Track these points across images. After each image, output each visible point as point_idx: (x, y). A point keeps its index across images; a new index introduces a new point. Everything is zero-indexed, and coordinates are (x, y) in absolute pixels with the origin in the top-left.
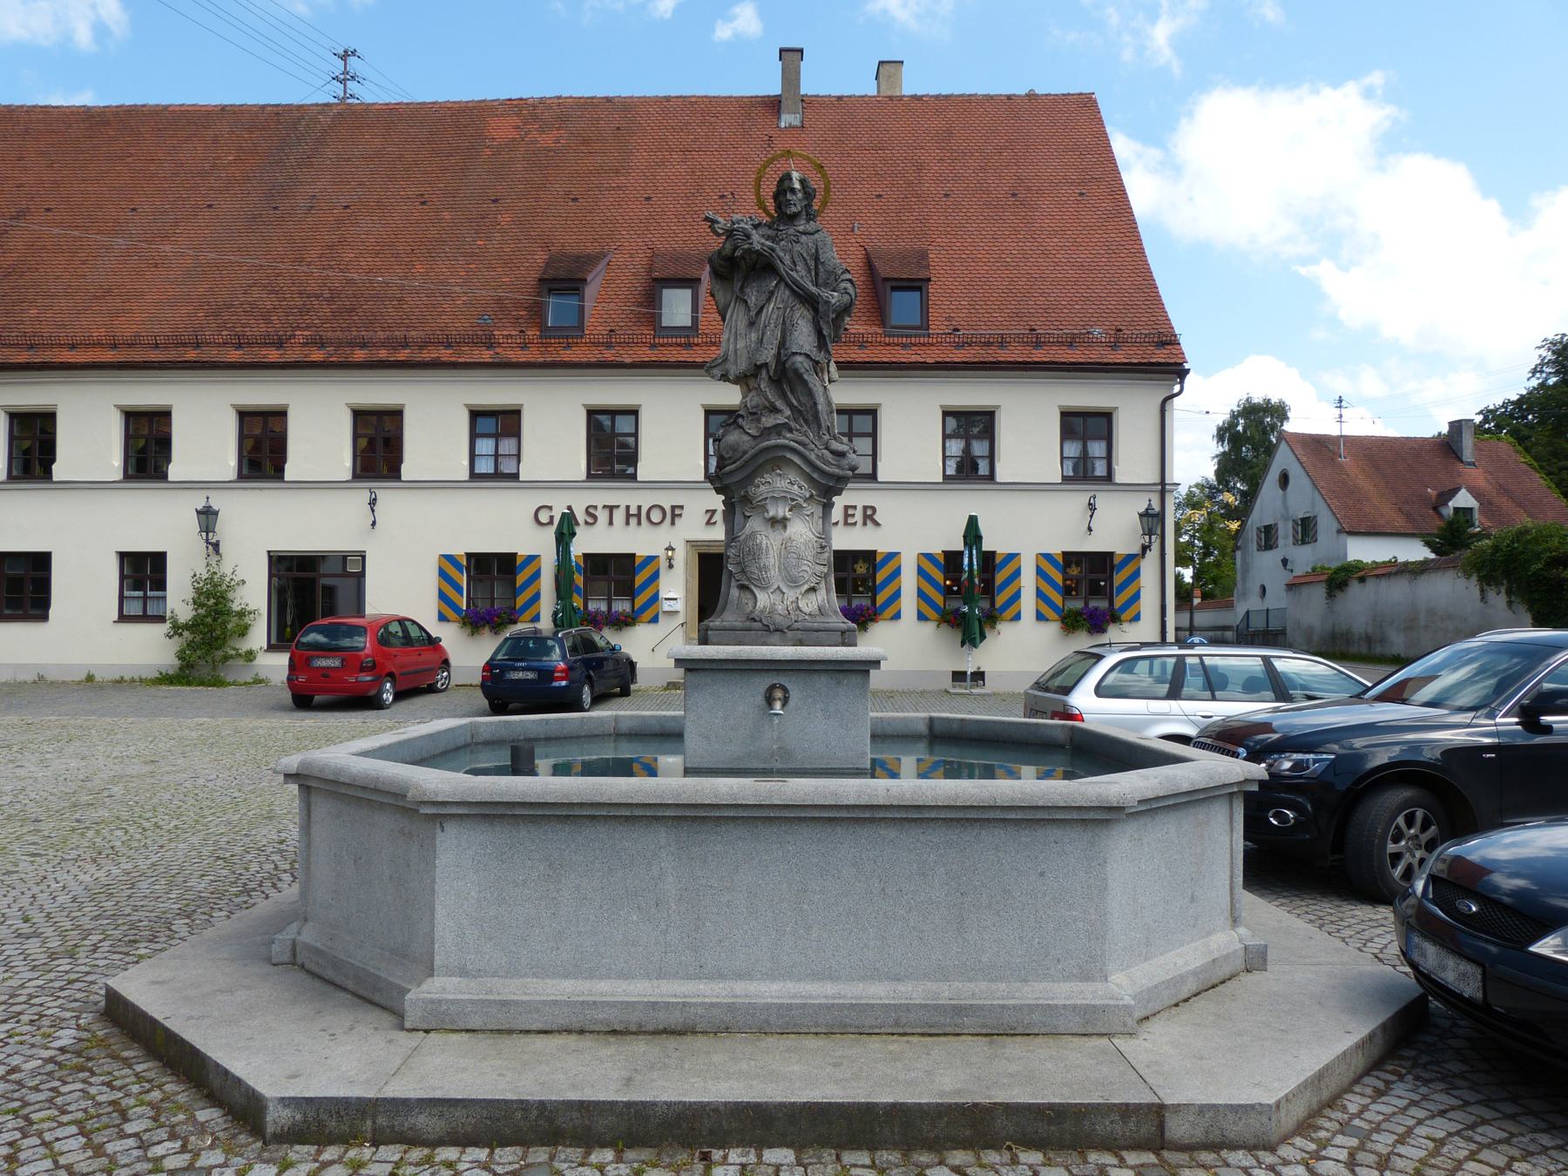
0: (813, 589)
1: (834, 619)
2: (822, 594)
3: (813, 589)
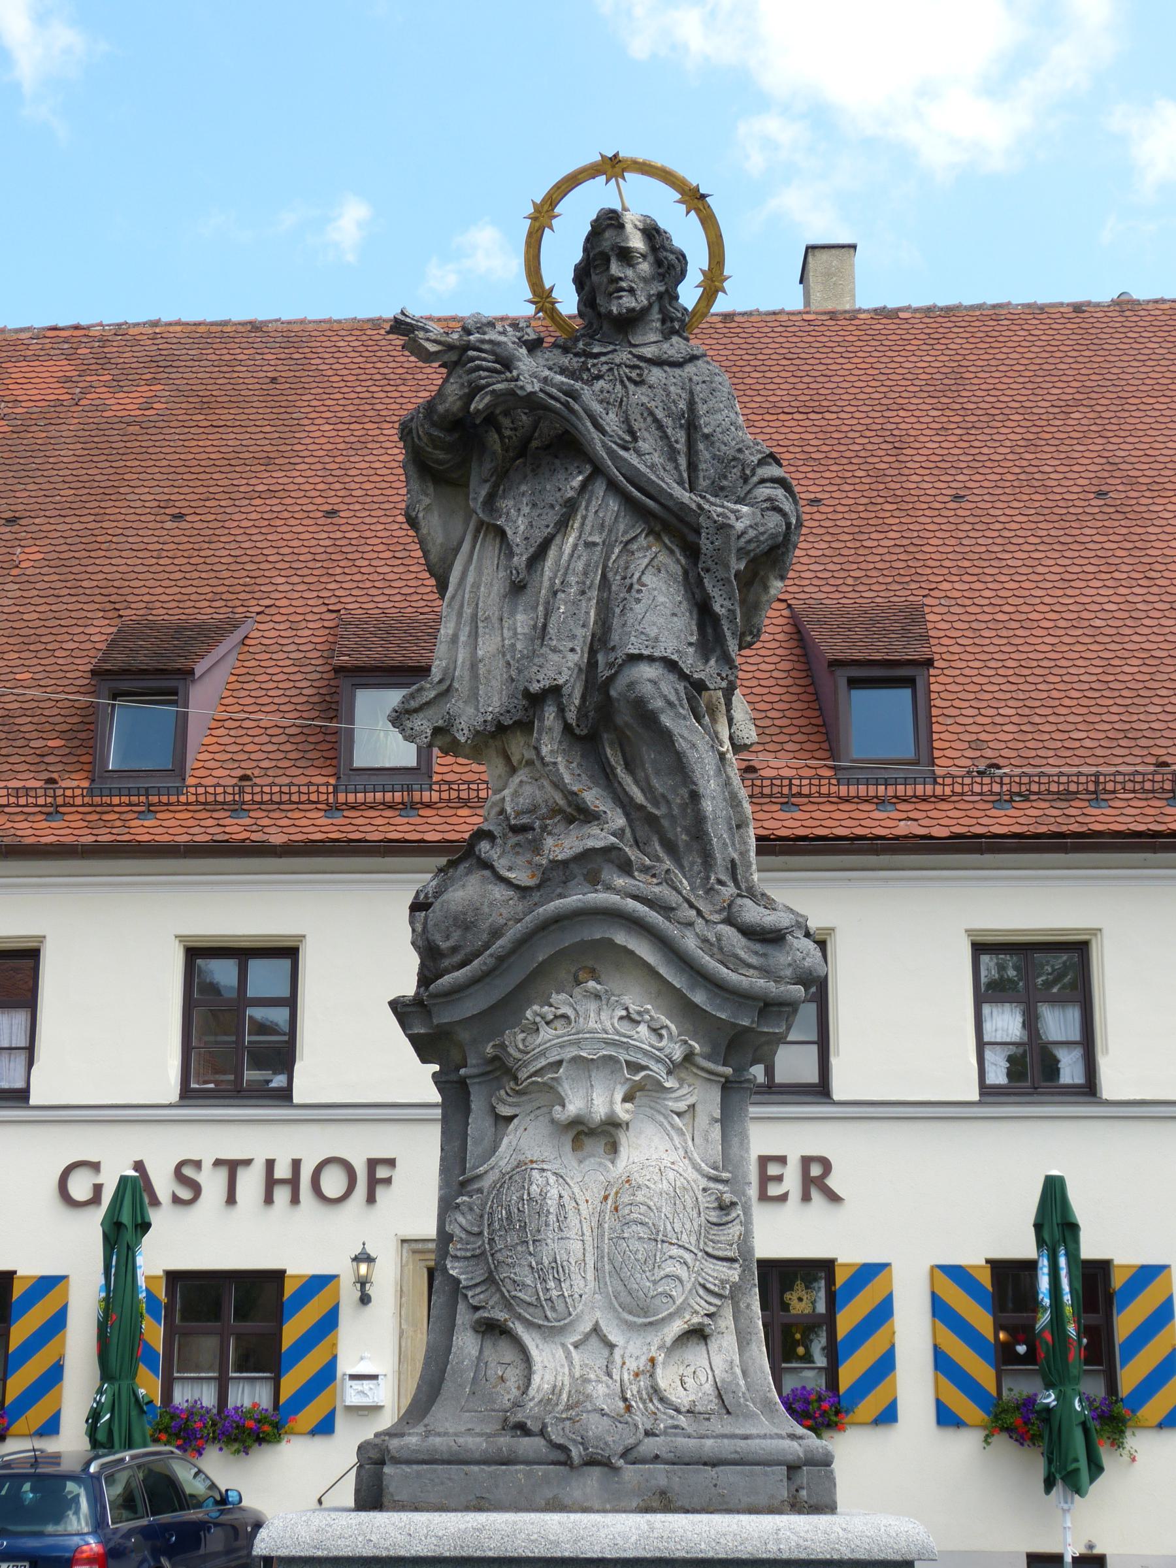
0: (698, 1334)
1: (764, 1425)
2: (725, 1346)
3: (698, 1334)
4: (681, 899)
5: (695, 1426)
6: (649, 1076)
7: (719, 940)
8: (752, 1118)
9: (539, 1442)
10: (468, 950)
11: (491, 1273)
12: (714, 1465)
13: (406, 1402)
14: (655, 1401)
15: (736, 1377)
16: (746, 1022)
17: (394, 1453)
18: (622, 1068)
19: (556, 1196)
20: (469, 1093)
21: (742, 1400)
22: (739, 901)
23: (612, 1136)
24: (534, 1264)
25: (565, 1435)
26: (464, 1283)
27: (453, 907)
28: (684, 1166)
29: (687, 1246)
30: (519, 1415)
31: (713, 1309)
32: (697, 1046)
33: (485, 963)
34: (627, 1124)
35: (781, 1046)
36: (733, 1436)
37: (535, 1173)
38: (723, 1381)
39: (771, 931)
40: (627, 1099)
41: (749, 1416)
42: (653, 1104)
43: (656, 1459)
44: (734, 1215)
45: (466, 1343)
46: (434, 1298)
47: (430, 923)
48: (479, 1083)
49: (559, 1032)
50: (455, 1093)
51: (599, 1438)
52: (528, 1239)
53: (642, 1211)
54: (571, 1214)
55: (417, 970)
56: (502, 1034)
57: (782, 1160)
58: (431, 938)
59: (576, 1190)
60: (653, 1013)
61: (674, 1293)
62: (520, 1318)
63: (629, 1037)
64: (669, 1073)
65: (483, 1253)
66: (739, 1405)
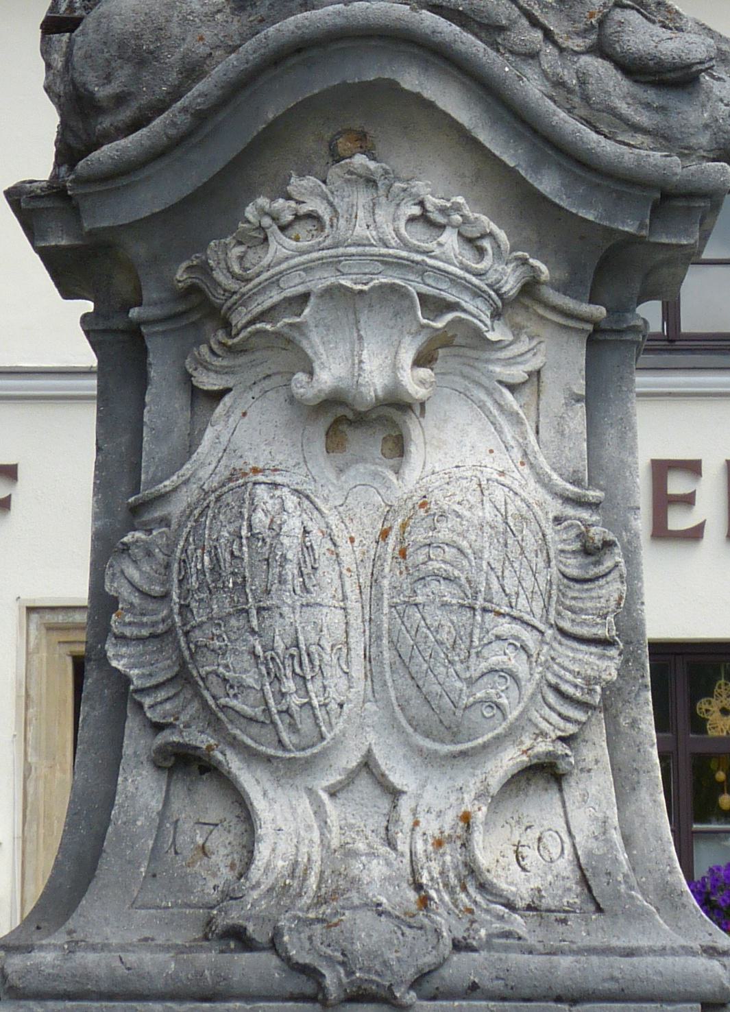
0: (546, 773)
1: (662, 932)
2: (591, 800)
3: (546, 773)
4: (516, 12)
5: (540, 933)
6: (461, 320)
7: (583, 82)
8: (640, 395)
9: (267, 960)
10: (144, 100)
11: (183, 665)
12: (574, 1001)
13: (36, 890)
14: (471, 890)
15: (613, 848)
16: (629, 228)
17: (14, 979)
18: (413, 307)
19: (299, 531)
20: (144, 351)
21: (623, 888)
22: (618, 15)
23: (395, 425)
24: (259, 649)
25: (313, 949)
26: (137, 683)
27: (117, 26)
28: (521, 478)
29: (527, 617)
30: (234, 914)
31: (571, 729)
32: (543, 268)
33: (173, 124)
34: (422, 405)
35: (692, 269)
36: (607, 951)
37: (261, 491)
38: (590, 854)
39: (675, 68)
40: (423, 360)
41: (635, 915)
42: (466, 370)
43: (473, 990)
44: (608, 564)
45: (140, 788)
46: (84, 709)
47: (78, 54)
48: (164, 332)
49: (303, 244)
50: (122, 350)
51: (372, 954)
52: (250, 608)
53: (448, 557)
54: (324, 563)
55: (54, 137)
56: (204, 247)
57: (693, 468)
58: (79, 79)
59: (333, 520)
60: (467, 211)
61: (504, 701)
62: (235, 743)
63: (426, 253)
64: (496, 315)
65: (171, 631)
66: (618, 896)
